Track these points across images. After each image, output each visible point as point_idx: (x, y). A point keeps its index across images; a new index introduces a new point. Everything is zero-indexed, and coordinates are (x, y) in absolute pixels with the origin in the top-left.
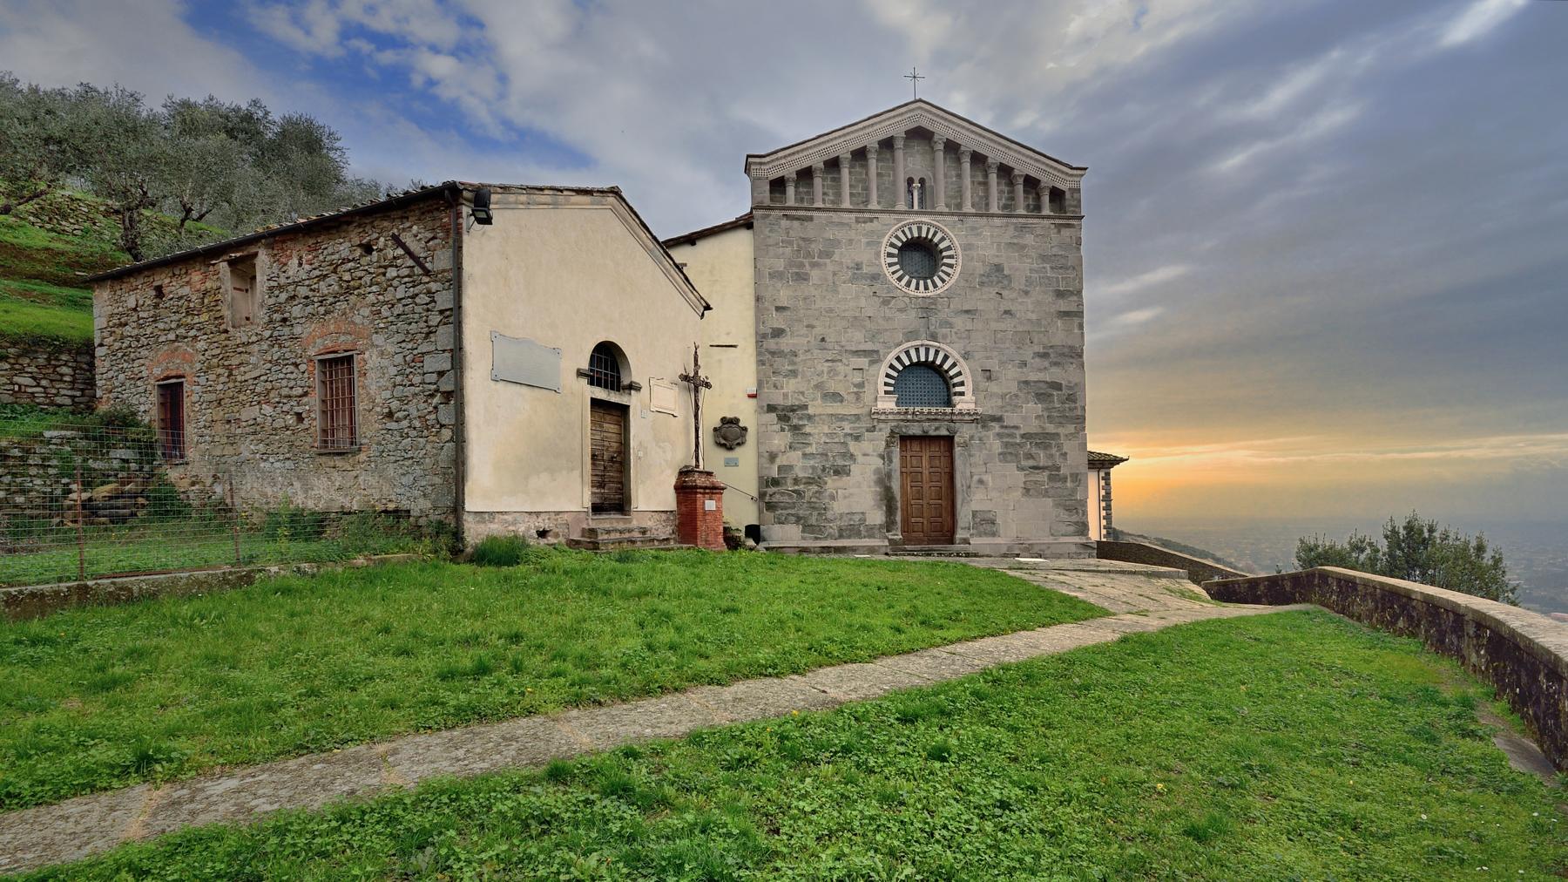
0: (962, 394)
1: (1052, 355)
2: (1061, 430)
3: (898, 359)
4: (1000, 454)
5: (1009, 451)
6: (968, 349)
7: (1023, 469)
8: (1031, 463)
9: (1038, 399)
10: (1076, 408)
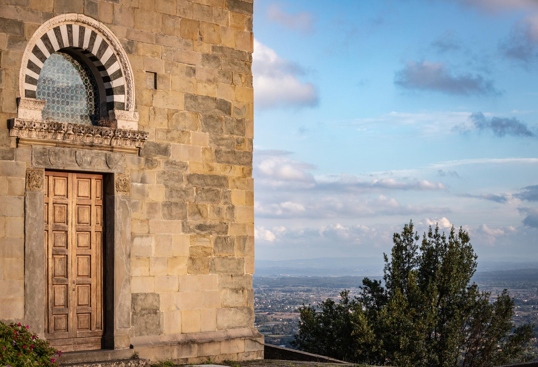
0: (122, 106)
1: (223, 61)
2: (226, 173)
3: (45, 38)
4: (165, 205)
5: (173, 200)
6: (133, 36)
7: (191, 231)
8: (200, 221)
9: (206, 124)
10: (243, 141)
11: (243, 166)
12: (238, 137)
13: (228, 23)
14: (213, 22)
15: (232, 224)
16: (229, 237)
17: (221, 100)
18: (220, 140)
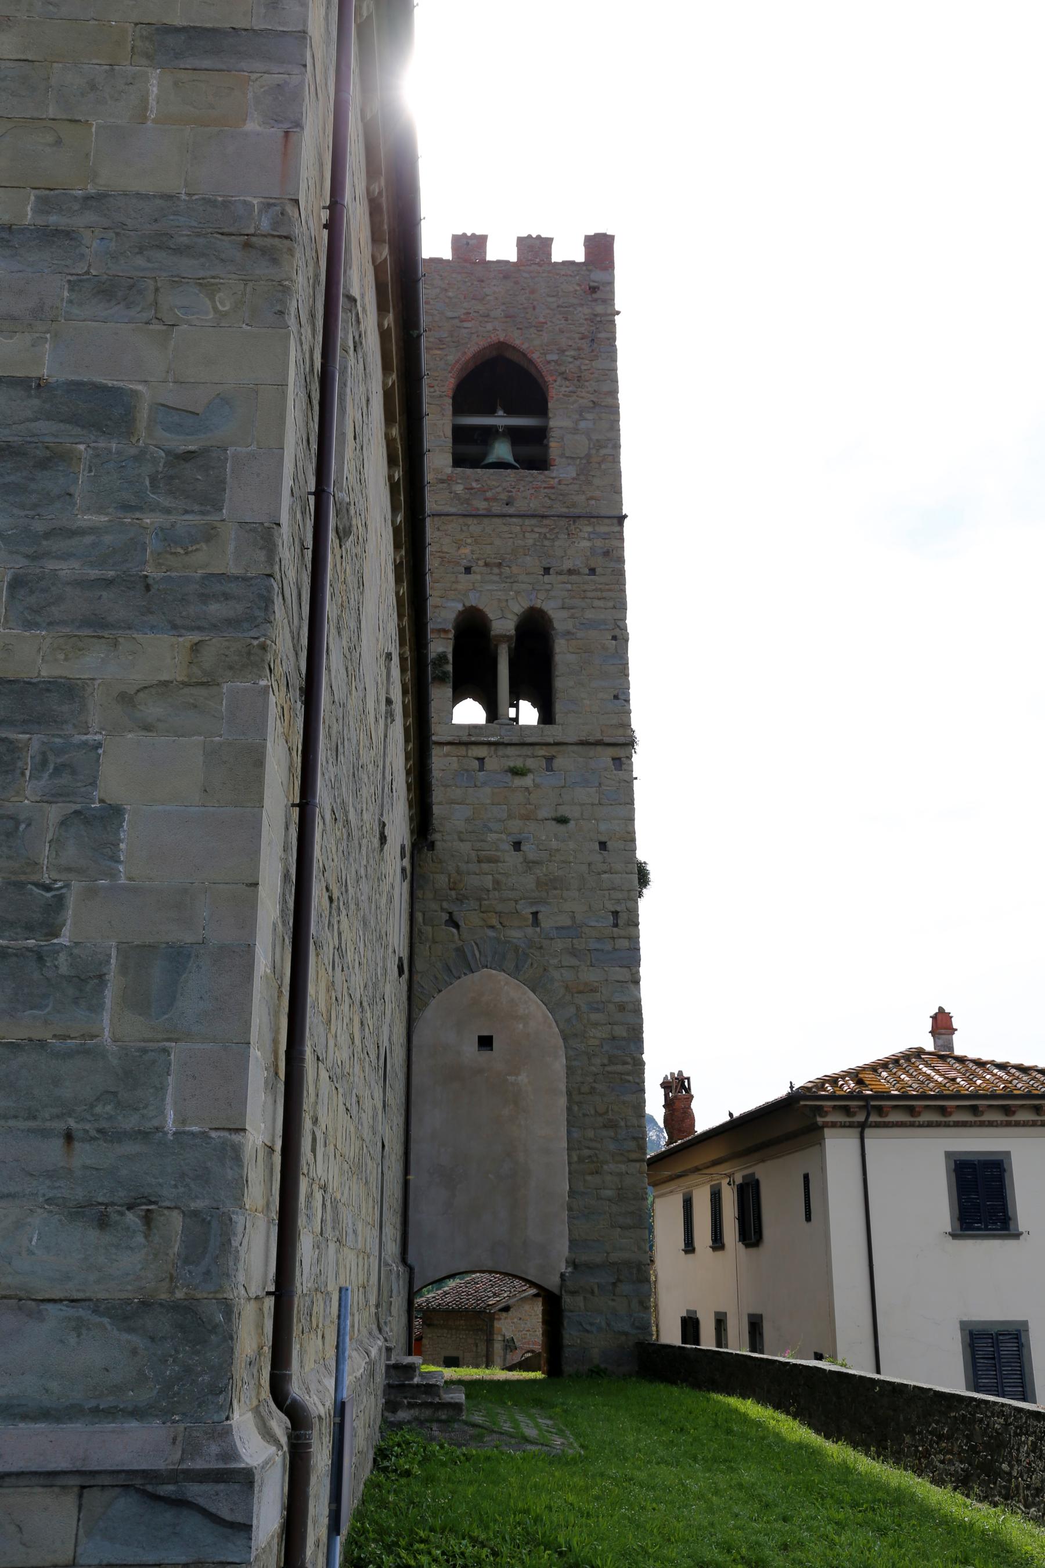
11: (195, 637)
12: (172, 518)
13: (145, 109)
14: (52, 111)
15: (91, 893)
16: (63, 947)
17: (79, 384)
18: (48, 535)
